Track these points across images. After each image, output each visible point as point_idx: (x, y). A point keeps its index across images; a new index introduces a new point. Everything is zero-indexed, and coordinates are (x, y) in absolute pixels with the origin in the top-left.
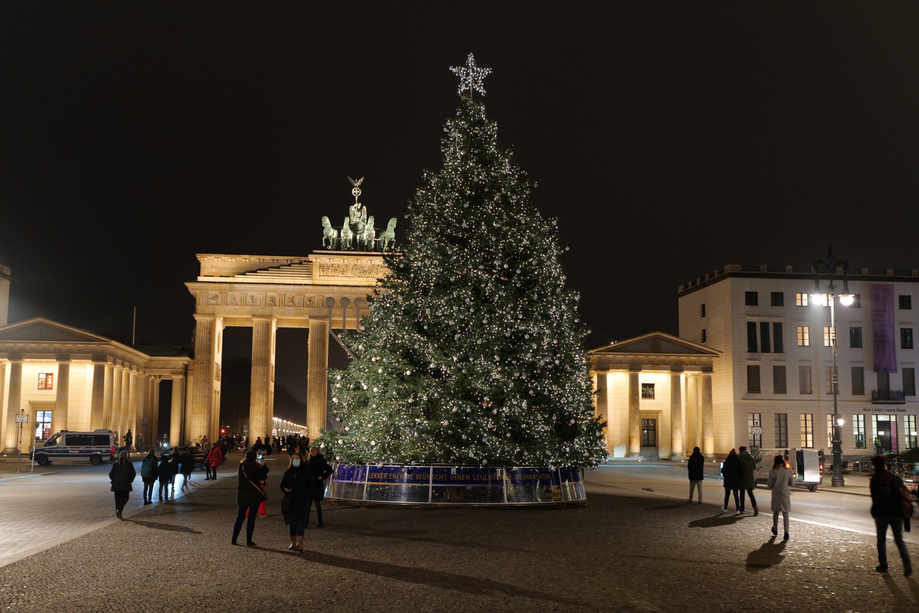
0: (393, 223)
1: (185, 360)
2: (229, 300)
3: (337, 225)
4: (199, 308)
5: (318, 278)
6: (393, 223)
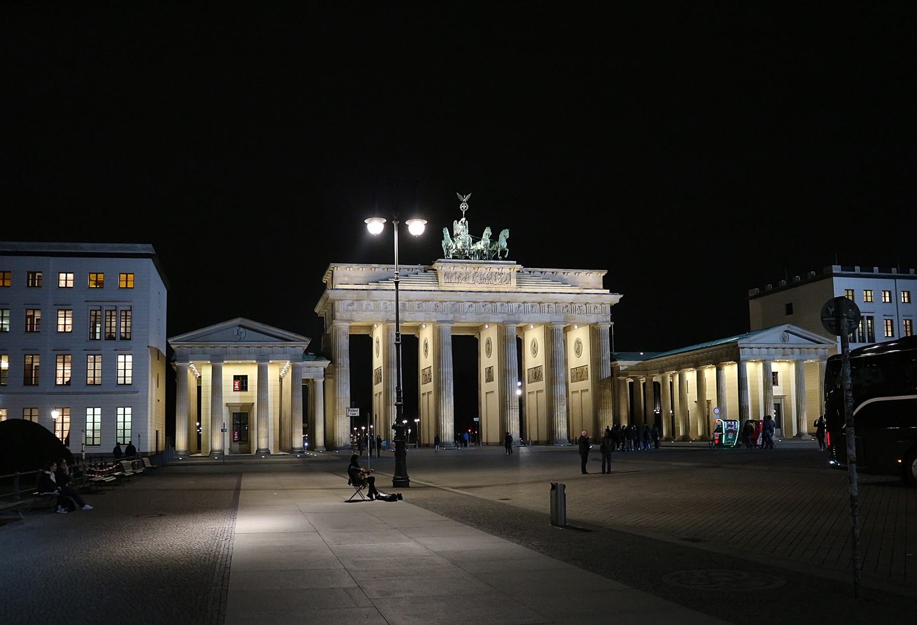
0: (505, 234)
1: (326, 363)
2: (364, 307)
4: (338, 315)
5: (444, 284)
6: (505, 234)
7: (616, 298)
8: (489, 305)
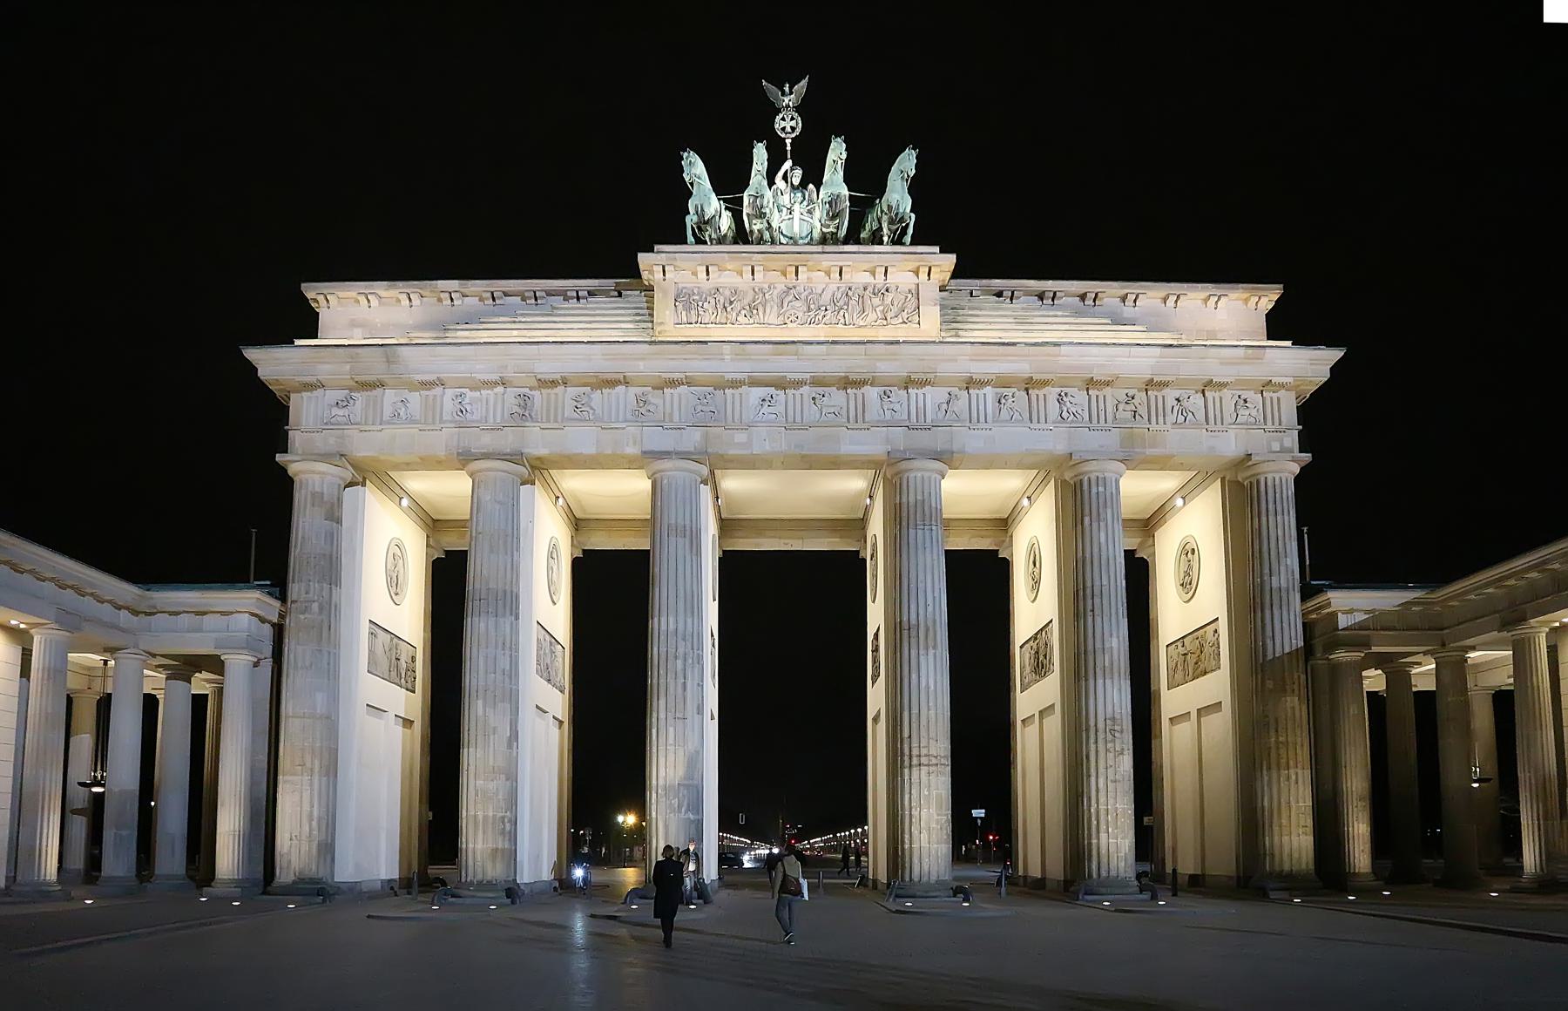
2: (388, 412)
3: (730, 182)
4: (296, 438)
7: (1312, 365)
8: (837, 398)
